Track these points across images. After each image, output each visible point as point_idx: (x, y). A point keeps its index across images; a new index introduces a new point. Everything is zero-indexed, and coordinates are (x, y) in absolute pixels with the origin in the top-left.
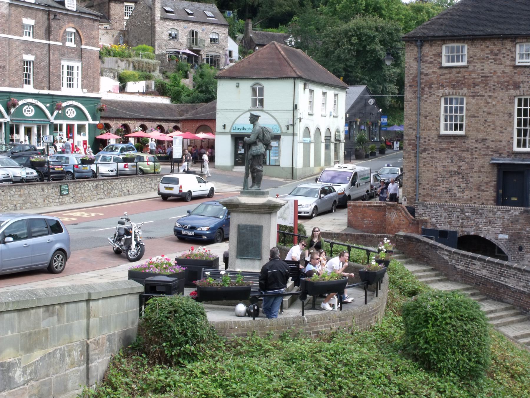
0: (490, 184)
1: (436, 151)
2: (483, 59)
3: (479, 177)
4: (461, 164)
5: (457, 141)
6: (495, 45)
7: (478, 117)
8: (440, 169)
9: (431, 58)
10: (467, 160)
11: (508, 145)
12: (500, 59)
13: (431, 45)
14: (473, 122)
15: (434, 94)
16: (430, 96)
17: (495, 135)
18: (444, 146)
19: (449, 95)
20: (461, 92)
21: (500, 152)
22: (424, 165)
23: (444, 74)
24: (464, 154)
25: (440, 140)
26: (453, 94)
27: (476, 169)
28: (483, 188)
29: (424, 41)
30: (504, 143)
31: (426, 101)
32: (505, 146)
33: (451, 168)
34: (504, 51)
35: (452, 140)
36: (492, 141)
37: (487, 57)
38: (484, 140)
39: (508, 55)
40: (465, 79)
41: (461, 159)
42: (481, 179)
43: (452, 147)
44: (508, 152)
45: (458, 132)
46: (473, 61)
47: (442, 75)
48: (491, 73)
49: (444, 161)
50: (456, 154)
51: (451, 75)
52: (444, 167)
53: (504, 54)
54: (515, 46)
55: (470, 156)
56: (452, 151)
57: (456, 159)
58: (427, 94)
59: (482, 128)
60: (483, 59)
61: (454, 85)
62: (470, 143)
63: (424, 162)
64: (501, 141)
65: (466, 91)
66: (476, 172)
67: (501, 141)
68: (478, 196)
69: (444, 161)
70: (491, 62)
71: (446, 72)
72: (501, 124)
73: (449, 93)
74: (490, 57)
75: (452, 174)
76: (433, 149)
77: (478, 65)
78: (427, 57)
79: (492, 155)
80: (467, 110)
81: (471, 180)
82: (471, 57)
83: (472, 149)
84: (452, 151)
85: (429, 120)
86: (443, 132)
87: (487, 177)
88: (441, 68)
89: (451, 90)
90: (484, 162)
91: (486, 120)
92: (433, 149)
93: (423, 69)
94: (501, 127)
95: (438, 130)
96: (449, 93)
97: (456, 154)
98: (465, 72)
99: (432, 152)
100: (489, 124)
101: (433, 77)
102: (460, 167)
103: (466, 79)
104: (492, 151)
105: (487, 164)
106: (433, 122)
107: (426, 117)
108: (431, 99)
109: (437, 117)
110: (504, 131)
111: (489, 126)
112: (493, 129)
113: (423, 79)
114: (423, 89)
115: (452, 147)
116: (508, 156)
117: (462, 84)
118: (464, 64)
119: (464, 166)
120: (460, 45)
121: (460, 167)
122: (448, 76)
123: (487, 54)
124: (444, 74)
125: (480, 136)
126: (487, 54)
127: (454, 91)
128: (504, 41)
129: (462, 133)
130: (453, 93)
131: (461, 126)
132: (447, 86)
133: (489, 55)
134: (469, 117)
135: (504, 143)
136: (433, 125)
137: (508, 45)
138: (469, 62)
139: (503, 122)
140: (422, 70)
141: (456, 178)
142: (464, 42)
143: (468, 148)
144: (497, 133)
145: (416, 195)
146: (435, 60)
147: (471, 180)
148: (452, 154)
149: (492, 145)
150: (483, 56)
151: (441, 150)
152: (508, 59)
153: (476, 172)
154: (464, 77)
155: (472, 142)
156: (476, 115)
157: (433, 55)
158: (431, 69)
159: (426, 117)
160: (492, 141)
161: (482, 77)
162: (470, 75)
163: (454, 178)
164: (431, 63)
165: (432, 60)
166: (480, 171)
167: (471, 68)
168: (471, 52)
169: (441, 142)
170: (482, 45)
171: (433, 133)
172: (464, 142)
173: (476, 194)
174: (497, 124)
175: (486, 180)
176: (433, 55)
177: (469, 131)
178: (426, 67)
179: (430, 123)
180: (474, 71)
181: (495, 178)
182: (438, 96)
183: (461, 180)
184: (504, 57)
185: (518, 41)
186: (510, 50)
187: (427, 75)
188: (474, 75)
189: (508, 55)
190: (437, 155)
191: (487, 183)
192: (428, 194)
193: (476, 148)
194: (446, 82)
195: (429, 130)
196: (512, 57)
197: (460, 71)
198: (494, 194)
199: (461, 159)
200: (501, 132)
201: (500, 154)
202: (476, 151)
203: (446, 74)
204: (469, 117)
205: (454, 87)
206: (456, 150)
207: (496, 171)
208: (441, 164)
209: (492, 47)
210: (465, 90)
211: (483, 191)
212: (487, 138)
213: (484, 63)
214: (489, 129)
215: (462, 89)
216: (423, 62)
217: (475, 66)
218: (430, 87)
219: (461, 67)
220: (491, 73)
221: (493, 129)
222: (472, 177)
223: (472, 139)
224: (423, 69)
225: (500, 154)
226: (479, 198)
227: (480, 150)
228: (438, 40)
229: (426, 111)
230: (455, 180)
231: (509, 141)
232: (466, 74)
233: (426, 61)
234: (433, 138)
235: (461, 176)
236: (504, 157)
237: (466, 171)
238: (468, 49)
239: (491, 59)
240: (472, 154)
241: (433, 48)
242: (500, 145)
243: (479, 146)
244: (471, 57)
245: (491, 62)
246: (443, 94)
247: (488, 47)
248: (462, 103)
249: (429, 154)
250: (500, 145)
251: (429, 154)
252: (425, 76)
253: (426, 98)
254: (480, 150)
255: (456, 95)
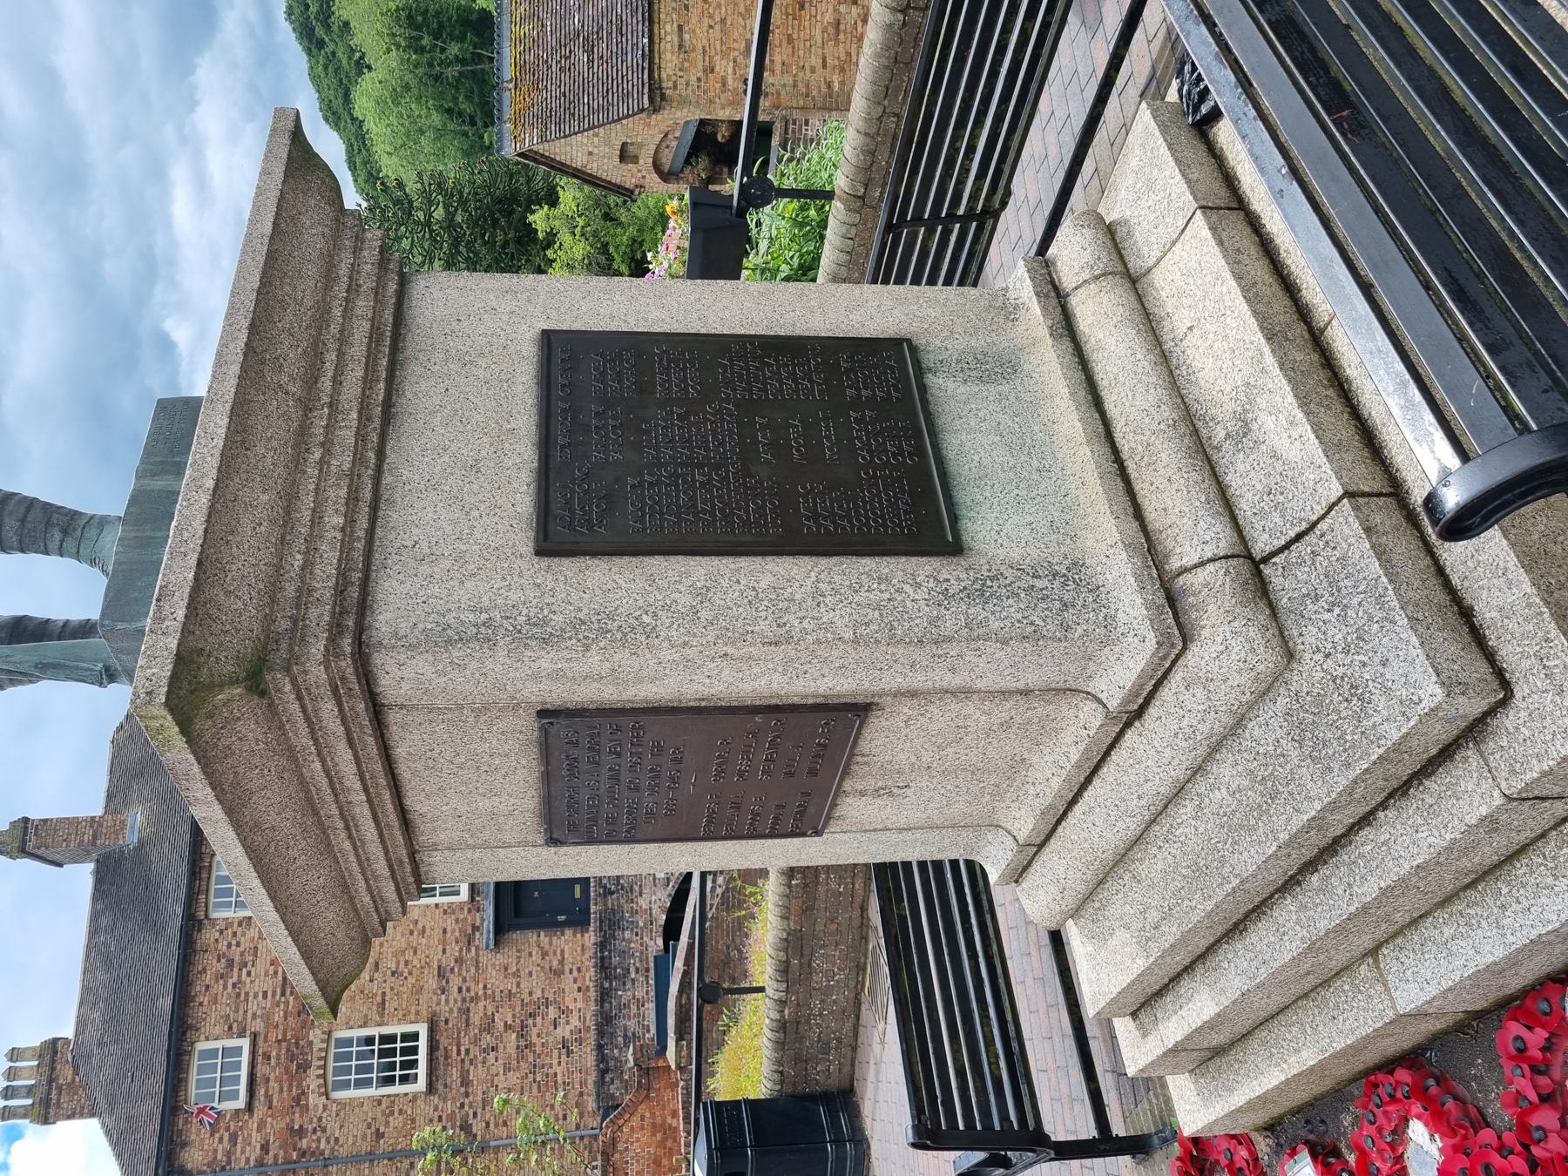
0: (547, 947)
1: (467, 1095)
2: (238, 995)
3: (530, 974)
4: (500, 1025)
5: (443, 1041)
6: (204, 970)
7: (384, 994)
8: (513, 1078)
9: (221, 1140)
10: (490, 1010)
11: (453, 912)
12: (242, 954)
13: (184, 1144)
14: (396, 1004)
15: (320, 1119)
16: (324, 1130)
17: (429, 947)
18: (455, 1074)
19: (324, 1076)
20: (318, 1045)
21: (469, 930)
22: (505, 1124)
23: (269, 1098)
24: (476, 1019)
25: (441, 1088)
26: (324, 1067)
27: (510, 985)
28: (555, 963)
29: (171, 1165)
30: (450, 923)
31: (337, 1140)
32: (457, 921)
33: (511, 1049)
34: (222, 946)
35: (440, 1054)
36: (444, 951)
37: (234, 986)
38: (441, 973)
39: (235, 934)
40: (284, 1039)
41: (488, 1027)
42: (535, 969)
43: (459, 1053)
44: (469, 911)
45: (422, 1044)
46: (240, 1024)
47: (271, 1102)
48: (276, 972)
49: (493, 1070)
50: (476, 1041)
51: (272, 1077)
52: (507, 1068)
53: (229, 945)
54: (213, 922)
55: (481, 1004)
56: (467, 1051)
57: (487, 1040)
58: (319, 1140)
59: (411, 980)
60: (240, 998)
61: (299, 1066)
62: (448, 1007)
63: (496, 1125)
64: (445, 931)
65: (318, 1031)
66: (518, 985)
67: (445, 931)
68: (575, 973)
69: (493, 1070)
70: (249, 974)
71: (262, 1091)
72: (403, 935)
73: (318, 1076)
74: (235, 979)
75: (526, 1046)
76: (462, 1105)
77: (253, 1007)
78: (215, 1151)
79: (477, 948)
80: (365, 1025)
81: (539, 993)
82: (230, 1028)
83: (464, 1000)
84: (467, 1051)
85: (387, 1123)
86: (421, 1085)
87: (530, 954)
88: (250, 1107)
89: (314, 1072)
90: (494, 965)
91: (393, 974)
92: (462, 1105)
93: (248, 1160)
94: (412, 933)
95: (415, 1097)
96: (318, 1076)
97: (476, 1041)
98: (266, 1037)
99: (471, 1107)
100: (402, 965)
101: (275, 1126)
102: (507, 1027)
103: (285, 1035)
104: (469, 950)
105: (500, 959)
106: (392, 1113)
107: (379, 1135)
108: (333, 1127)
109: (380, 1103)
110: (420, 925)
111: (407, 963)
112: (415, 952)
113: (276, 1157)
114: (303, 1154)
115: (459, 1053)
116: (478, 910)
117: (297, 1043)
118: (245, 1043)
119: (506, 1015)
120: (195, 1063)
121: (507, 1027)
122: (274, 1085)
123: (225, 987)
124: (269, 1098)
125: (432, 983)
126: (225, 987)
127: (316, 1063)
128: (198, 947)
129: (423, 1030)
130: (319, 1067)
131: (407, 1037)
132: (299, 1086)
133: (230, 982)
134: (382, 1016)
135: (450, 923)
136: (401, 1112)
137: (208, 936)
138: (241, 1035)
139: (399, 929)
140: (252, 1163)
141: (535, 1031)
142: (190, 1053)
143: (460, 1010)
144: (424, 941)
145: (582, 1138)
146: (227, 1129)
147: (539, 993)
148: (475, 1051)
149: (454, 950)
150: (230, 997)
151: (465, 1082)
152: (244, 934)
153: (518, 985)
154: (279, 1042)
155: (447, 1001)
156: (379, 999)
157: (212, 1135)
158: (250, 1135)
159: (379, 1135)
160: (444, 951)
161: (283, 994)
162: (277, 1027)
163: (535, 1039)
164: (233, 1139)
165: (226, 1138)
166: (517, 974)
167: (258, 1026)
168: (217, 1030)
169: (445, 1086)
170: (201, 1004)
171: (424, 1108)
172: (447, 1022)
173: (571, 978)
174: (404, 945)
175: (536, 957)
176: (212, 1135)
177: (417, 1013)
178: (243, 1152)
179: (396, 1121)
180: (267, 1018)
181: (532, 936)
182: (325, 1107)
183: (539, 1019)
184: (238, 945)
185: (201, 915)
186: (221, 932)
187: (265, 1148)
188: (278, 1016)
189: (235, 934)
190: (478, 1091)
191: (544, 954)
192: (577, 1105)
193: (460, 990)
194: (290, 1090)
195: (413, 1121)
196: (240, 924)
197: (264, 1054)
198: (568, 932)
199: (488, 1027)
200: (424, 931)
201: (475, 928)
202: (468, 990)
203: (267, 1091)
204: (382, 1016)
205: (304, 1067)
206: (465, 1041)
207: (516, 936)
208: (502, 1078)
209: (208, 978)
210: (316, 1036)
211: (562, 962)
212: (435, 966)
213: (247, 994)
214: (416, 962)
215: (311, 1043)
216: (229, 1163)
217: (254, 1016)
218: (301, 1132)
219: (253, 1053)
220: (276, 972)
221: (415, 952)
222: (530, 994)
223: (438, 1004)
224: (248, 1160)
225: (475, 928)
226: (579, 970)
227: (464, 980)
228: (174, 1124)
229: (364, 1137)
230: (538, 1035)
231: (445, 912)
232: (272, 1037)
233: (229, 1154)
234: (436, 1109)
235: (530, 1021)
236: (483, 920)
237: (518, 1009)
238: (207, 1039)
239: (240, 976)
240: (475, 999)
241: (193, 1137)
242: (453, 931)
243: (455, 982)
244: (230, 1028)
245: (249, 974)
246: (321, 1095)
247: (207, 987)
248: (348, 1042)
249: (475, 1115)
250: (453, 931)
251: (475, 1115)
252: (267, 1153)
253: (328, 1141)
254: (464, 980)
255: (325, 1059)
